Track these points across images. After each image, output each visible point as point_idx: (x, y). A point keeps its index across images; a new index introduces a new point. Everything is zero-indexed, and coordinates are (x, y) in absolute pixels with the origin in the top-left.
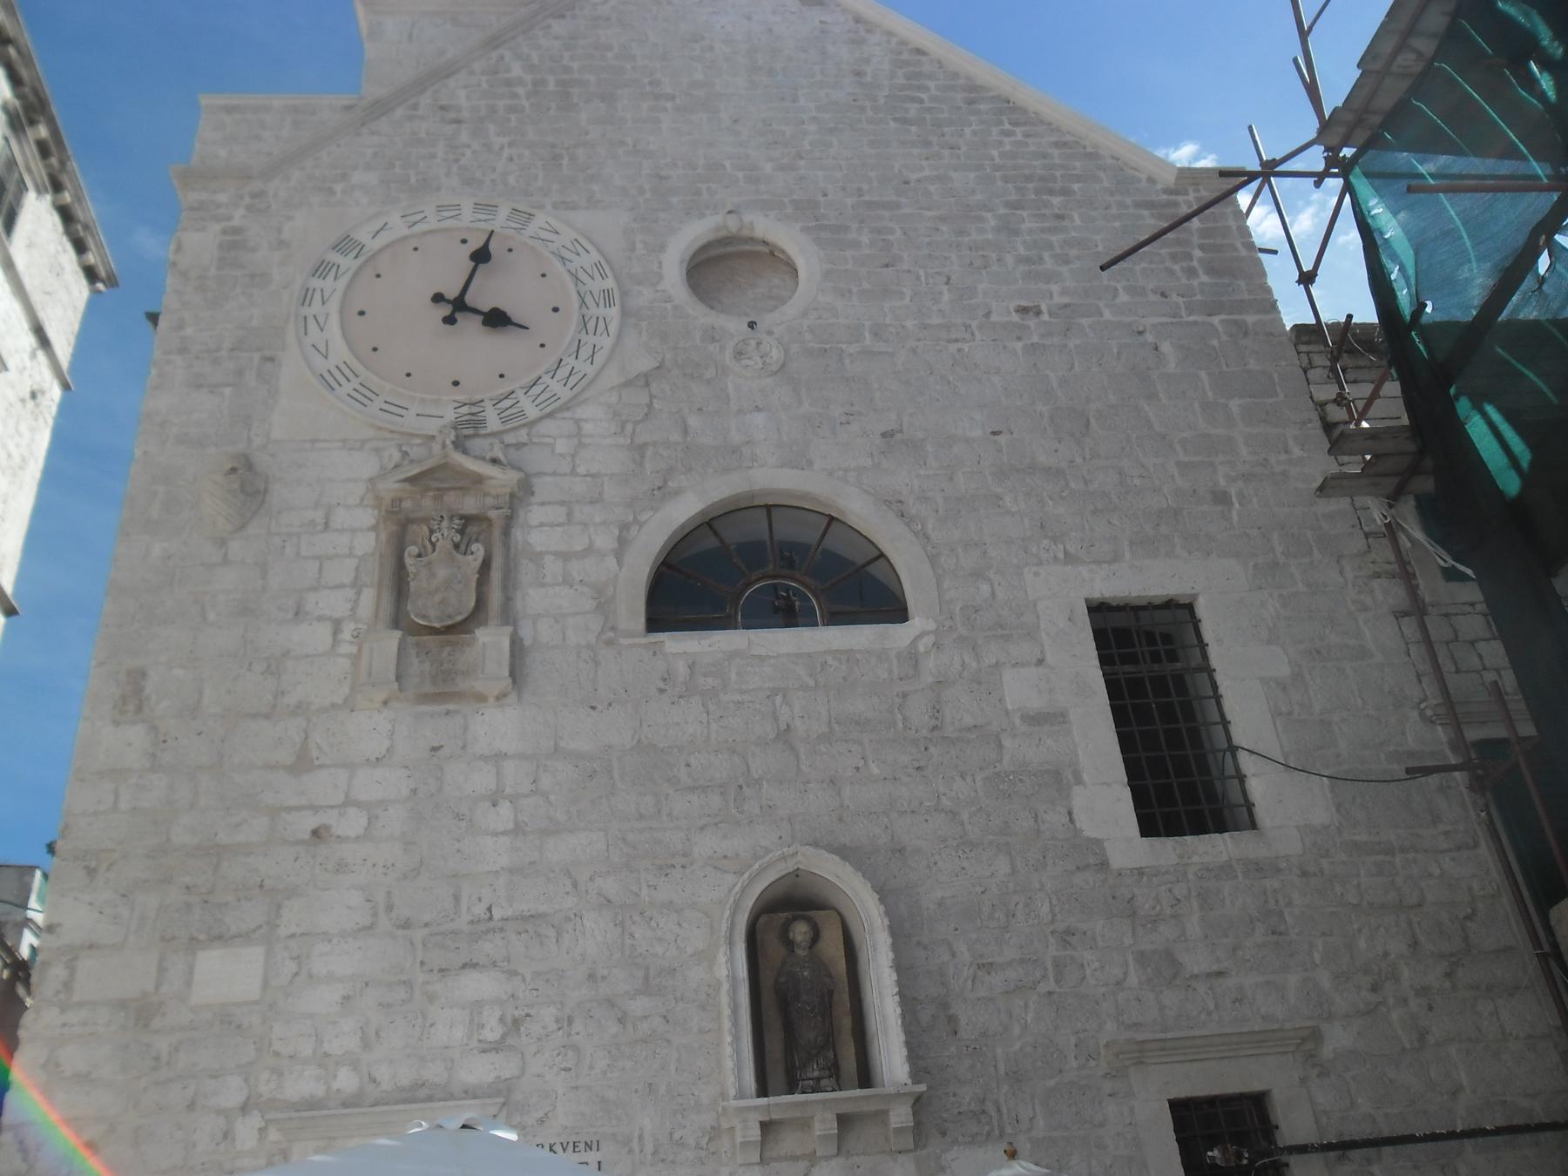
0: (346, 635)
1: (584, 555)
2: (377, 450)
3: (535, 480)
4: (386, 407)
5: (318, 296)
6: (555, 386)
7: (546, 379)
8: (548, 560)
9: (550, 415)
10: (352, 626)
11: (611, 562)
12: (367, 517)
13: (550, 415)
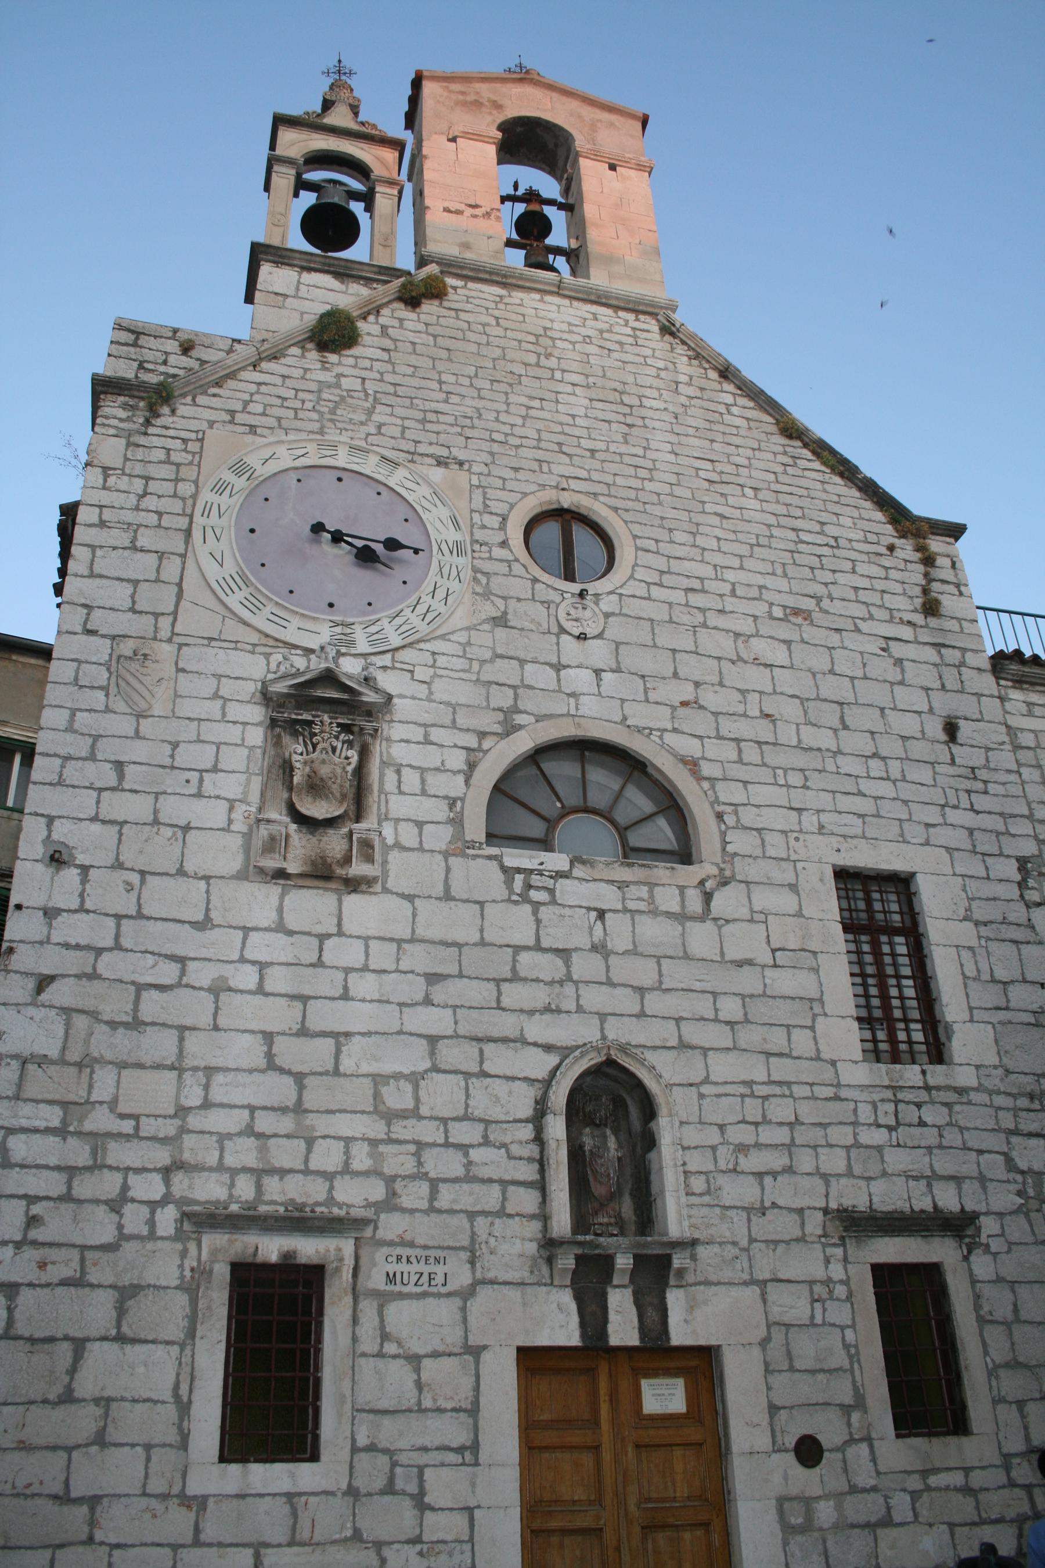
0: (238, 815)
2: (267, 656)
3: (395, 700)
5: (215, 508)
6: (415, 620)
7: (407, 612)
8: (405, 771)
9: (410, 645)
10: (244, 807)
11: (461, 779)
12: (257, 713)
13: (410, 645)
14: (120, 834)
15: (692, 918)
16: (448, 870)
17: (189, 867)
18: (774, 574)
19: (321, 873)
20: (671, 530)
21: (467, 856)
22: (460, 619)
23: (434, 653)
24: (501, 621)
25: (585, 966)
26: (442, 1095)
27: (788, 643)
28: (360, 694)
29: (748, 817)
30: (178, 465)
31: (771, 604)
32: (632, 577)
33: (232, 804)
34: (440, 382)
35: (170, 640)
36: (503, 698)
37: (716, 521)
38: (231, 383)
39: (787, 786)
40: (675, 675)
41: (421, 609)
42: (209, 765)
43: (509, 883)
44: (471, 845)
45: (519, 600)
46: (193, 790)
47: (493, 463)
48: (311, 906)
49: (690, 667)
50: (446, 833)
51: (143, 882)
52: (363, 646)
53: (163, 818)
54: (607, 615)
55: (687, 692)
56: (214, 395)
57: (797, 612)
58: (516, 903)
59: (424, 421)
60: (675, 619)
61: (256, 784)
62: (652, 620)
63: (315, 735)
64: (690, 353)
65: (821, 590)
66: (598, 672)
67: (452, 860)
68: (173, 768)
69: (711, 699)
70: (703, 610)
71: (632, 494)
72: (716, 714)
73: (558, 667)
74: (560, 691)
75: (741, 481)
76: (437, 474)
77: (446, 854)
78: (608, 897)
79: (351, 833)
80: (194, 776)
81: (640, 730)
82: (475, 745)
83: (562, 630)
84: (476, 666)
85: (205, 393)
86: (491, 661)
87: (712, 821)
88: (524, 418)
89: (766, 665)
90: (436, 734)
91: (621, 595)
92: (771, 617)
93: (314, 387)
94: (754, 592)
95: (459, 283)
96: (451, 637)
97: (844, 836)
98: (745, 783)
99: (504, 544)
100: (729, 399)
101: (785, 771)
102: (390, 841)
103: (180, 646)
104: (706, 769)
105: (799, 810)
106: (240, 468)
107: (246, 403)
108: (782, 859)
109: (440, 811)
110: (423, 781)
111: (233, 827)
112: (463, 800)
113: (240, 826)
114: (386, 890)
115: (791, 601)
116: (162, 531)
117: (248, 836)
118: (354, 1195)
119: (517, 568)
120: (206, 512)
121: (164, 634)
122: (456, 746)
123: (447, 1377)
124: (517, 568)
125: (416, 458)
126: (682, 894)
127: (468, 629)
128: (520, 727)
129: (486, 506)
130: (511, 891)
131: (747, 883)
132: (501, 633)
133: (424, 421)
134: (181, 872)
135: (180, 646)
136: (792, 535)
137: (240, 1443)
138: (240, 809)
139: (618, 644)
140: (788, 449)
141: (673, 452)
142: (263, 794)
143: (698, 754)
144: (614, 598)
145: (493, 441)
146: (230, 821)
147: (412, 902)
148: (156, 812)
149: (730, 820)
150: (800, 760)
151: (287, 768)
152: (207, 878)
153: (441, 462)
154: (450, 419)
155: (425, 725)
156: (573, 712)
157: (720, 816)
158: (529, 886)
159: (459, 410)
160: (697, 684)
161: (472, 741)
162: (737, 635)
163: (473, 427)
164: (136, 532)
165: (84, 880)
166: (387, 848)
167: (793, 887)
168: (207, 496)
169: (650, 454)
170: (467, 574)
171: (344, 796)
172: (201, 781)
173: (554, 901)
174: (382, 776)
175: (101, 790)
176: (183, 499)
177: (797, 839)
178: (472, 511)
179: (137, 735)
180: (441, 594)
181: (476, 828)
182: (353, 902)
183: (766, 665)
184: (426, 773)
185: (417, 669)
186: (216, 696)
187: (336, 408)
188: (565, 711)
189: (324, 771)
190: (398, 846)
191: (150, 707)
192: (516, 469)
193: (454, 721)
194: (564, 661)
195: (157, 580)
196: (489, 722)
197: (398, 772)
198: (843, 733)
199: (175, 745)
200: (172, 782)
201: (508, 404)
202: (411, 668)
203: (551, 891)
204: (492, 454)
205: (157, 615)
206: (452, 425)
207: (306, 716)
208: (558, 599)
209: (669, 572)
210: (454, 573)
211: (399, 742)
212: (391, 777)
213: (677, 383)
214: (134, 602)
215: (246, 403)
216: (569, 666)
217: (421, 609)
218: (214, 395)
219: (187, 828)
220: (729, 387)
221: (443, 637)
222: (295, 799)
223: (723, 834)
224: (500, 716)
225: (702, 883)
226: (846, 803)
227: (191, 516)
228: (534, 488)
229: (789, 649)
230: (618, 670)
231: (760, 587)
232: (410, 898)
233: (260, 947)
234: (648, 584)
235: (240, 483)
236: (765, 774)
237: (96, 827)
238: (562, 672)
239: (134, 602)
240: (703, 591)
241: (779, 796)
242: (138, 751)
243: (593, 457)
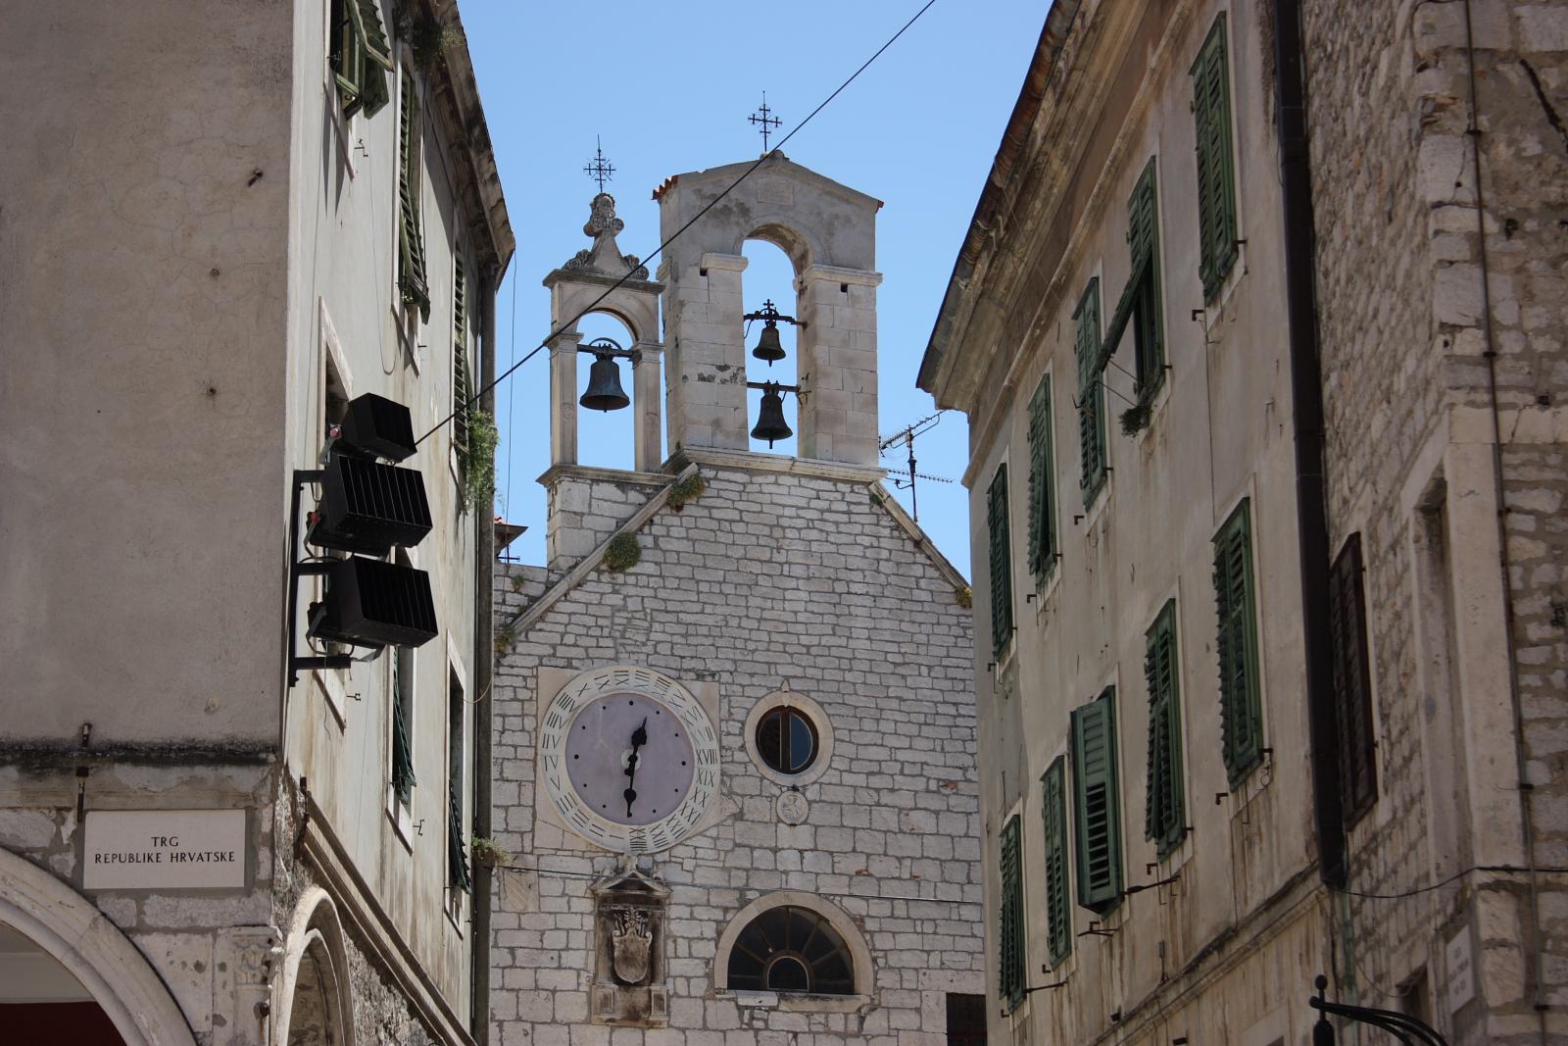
0: (583, 980)
4: (594, 829)
8: (680, 941)
10: (586, 974)
11: (713, 944)
12: (587, 905)
14: (517, 997)
15: (852, 1036)
16: (705, 1010)
17: (558, 1017)
18: (934, 750)
19: (635, 1017)
20: (861, 719)
21: (714, 999)
22: (712, 818)
23: (695, 848)
24: (739, 816)
27: (937, 813)
28: (653, 890)
29: (893, 960)
30: (522, 701)
31: (929, 779)
32: (830, 767)
33: (578, 971)
34: (698, 593)
35: (532, 853)
36: (739, 880)
37: (895, 704)
38: (551, 617)
39: (923, 933)
40: (854, 850)
41: (687, 812)
42: (563, 946)
43: (741, 1016)
44: (719, 991)
45: (752, 796)
46: (556, 965)
47: (736, 670)
49: (868, 842)
50: (704, 983)
51: (533, 1029)
52: (651, 847)
53: (541, 984)
54: (810, 803)
55: (860, 863)
56: (540, 630)
57: (948, 783)
58: (745, 1030)
59: (686, 636)
60: (858, 801)
61: (592, 955)
62: (841, 803)
63: (625, 922)
64: (893, 524)
65: (968, 761)
66: (801, 852)
67: (708, 1003)
68: (542, 949)
69: (877, 868)
70: (877, 790)
71: (834, 687)
72: (879, 879)
73: (775, 850)
74: (776, 869)
75: (920, 660)
76: (697, 687)
77: (704, 999)
78: (801, 1023)
79: (650, 992)
80: (555, 954)
81: (826, 896)
82: (721, 918)
83: (780, 821)
84: (722, 854)
85: (533, 629)
86: (733, 850)
87: (869, 964)
88: (759, 620)
89: (918, 835)
90: (699, 912)
91: (821, 784)
92: (928, 791)
93: (607, 611)
94: (916, 770)
95: (710, 474)
96: (708, 833)
97: (957, 970)
98: (894, 934)
99: (743, 748)
100: (918, 571)
101: (923, 921)
102: (671, 993)
103: (539, 856)
104: (870, 925)
105: (928, 952)
106: (565, 702)
107: (562, 636)
108: (913, 990)
109: (701, 971)
110: (690, 947)
111: (581, 988)
112: (714, 959)
113: (584, 988)
114: (670, 1026)
115: (943, 773)
116: (519, 763)
117: (589, 994)
119: (751, 769)
120: (545, 745)
121: (528, 849)
122: (709, 920)
124: (751, 769)
125: (682, 674)
126: (846, 1019)
127: (717, 825)
128: (751, 901)
129: (731, 714)
130: (742, 1023)
131: (888, 1008)
132: (739, 825)
133: (686, 636)
134: (554, 1021)
135: (539, 856)
136: (952, 710)
138: (584, 974)
139: (816, 827)
140: (963, 619)
141: (869, 639)
142: (596, 964)
143: (864, 913)
144: (817, 786)
145: (736, 648)
146: (579, 984)
147: (684, 1033)
148: (536, 981)
149: (881, 962)
150: (933, 912)
151: (610, 946)
152: (568, 1024)
153: (700, 677)
154: (704, 631)
155: (690, 906)
156: (784, 886)
157: (874, 960)
158: (752, 1018)
159: (710, 621)
160: (868, 856)
161: (719, 915)
162: (901, 810)
163: (721, 637)
164: (502, 764)
165: (501, 1031)
166: (670, 997)
167: (918, 1010)
168: (545, 729)
169: (853, 644)
170: (717, 779)
171: (644, 964)
172: (560, 957)
173: (767, 1028)
174: (665, 945)
175: (504, 968)
176: (529, 732)
177: (925, 974)
178: (721, 720)
179: (520, 928)
180: (700, 798)
181: (721, 980)
182: (650, 1033)
183: (918, 835)
185: (686, 861)
186: (563, 894)
187: (625, 631)
188: (778, 886)
189: (632, 948)
190: (676, 995)
191: (526, 907)
192: (752, 675)
193: (708, 900)
194: (780, 846)
195: (520, 805)
196: (730, 899)
197: (675, 941)
198: (966, 888)
199: (543, 933)
200: (544, 959)
201: (747, 607)
202: (680, 860)
203: (766, 1021)
204: (735, 661)
205: (522, 834)
206: (706, 636)
207: (619, 907)
208: (778, 792)
209: (857, 759)
210: (709, 778)
211: (677, 923)
212: (670, 945)
213: (878, 561)
214: (507, 824)
215: (562, 636)
216: (783, 849)
217: (687, 812)
218: (540, 630)
219: (554, 991)
220: (920, 558)
221: (701, 834)
222: (616, 968)
223: (876, 973)
224: (737, 894)
225: (859, 1010)
226: (961, 944)
227: (536, 747)
228: (764, 691)
229: (937, 818)
230: (815, 849)
231: (922, 764)
232: (683, 1030)
234: (841, 771)
235: (565, 714)
236: (906, 925)
237: (504, 993)
238: (778, 854)
239: (507, 824)
240: (880, 773)
241: (913, 941)
242: (521, 939)
243: (808, 653)
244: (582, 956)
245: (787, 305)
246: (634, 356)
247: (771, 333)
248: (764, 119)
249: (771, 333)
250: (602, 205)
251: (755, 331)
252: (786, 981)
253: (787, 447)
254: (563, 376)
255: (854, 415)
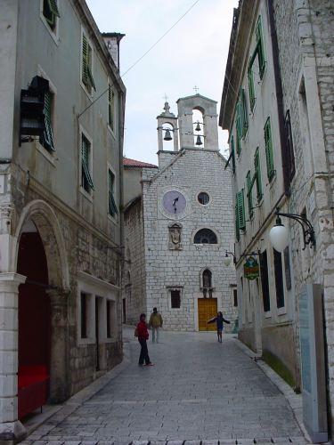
1: (188, 234)
19: (176, 249)
25: (205, 258)
26: (190, 273)
29: (225, 237)
48: (175, 253)
118: (182, 284)
123: (191, 301)
137: (173, 307)
184: (188, 234)
211: (184, 232)
233: (171, 258)
244: (167, 238)
245: (202, 121)
246: (173, 131)
247: (198, 126)
248: (195, 88)
249: (198, 126)
250: (166, 104)
251: (195, 126)
252: (205, 241)
253: (202, 146)
254: (160, 135)
255: (214, 140)
